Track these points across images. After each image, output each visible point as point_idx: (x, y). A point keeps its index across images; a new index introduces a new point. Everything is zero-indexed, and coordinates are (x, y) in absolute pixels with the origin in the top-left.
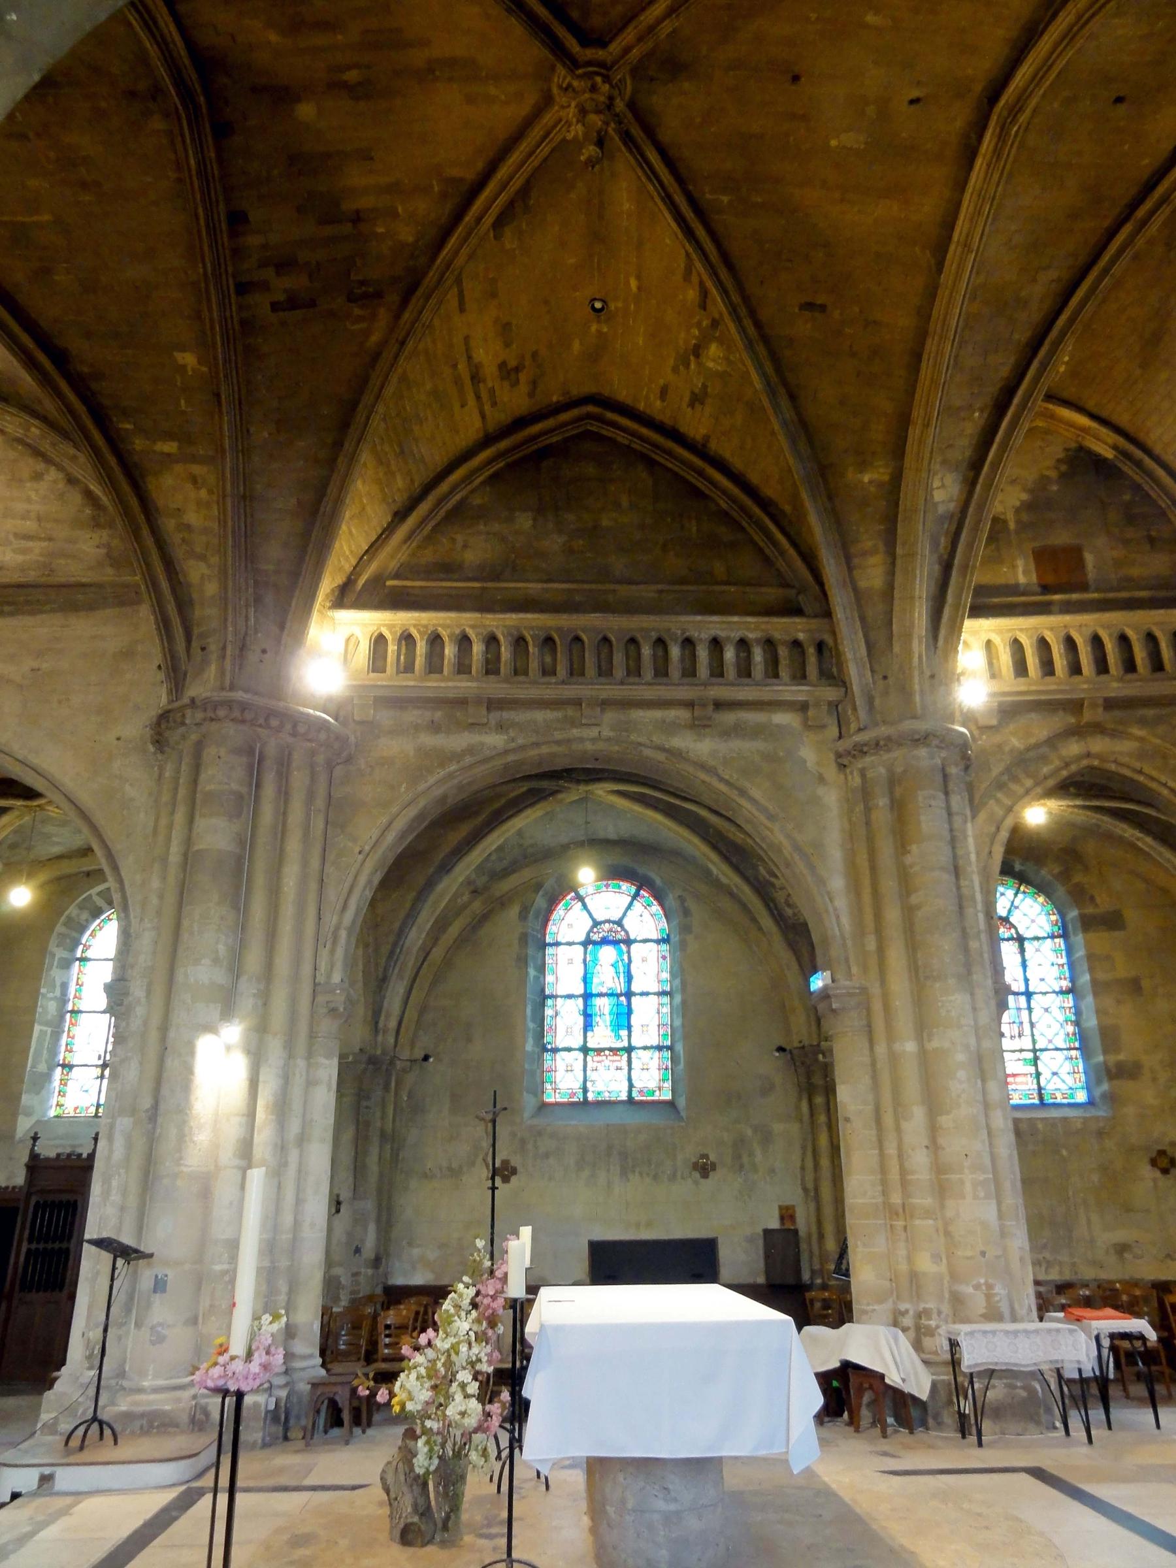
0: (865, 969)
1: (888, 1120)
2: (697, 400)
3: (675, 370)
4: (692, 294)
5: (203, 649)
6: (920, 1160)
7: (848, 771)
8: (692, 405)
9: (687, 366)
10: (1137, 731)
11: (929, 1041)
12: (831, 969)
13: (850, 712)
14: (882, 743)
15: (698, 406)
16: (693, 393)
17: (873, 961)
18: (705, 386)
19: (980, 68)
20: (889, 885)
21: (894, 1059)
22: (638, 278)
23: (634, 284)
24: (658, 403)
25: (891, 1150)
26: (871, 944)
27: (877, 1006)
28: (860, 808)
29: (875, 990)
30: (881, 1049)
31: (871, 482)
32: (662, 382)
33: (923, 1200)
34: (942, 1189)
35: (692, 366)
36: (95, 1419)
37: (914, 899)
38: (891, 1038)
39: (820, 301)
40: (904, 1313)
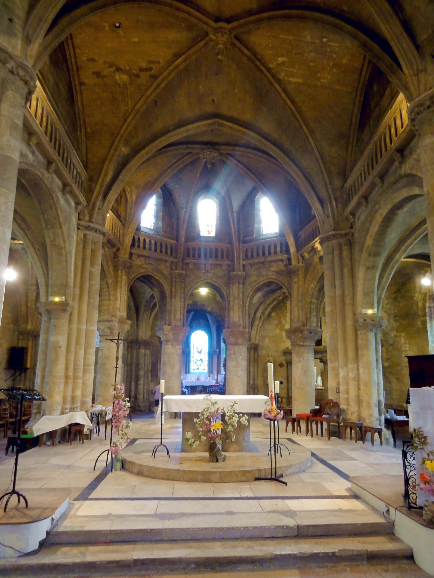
0: (73, 299)
1: (73, 349)
2: (98, 74)
3: (105, 63)
4: (144, 65)
5: (11, 20)
6: (82, 361)
7: (79, 231)
8: (94, 73)
9: (111, 66)
10: (107, 249)
11: (90, 326)
12: (65, 296)
13: (86, 213)
14: (98, 230)
15: (95, 76)
16: (99, 72)
17: (77, 297)
18: (106, 76)
19: (224, 111)
20: (87, 275)
21: (79, 330)
22: (138, 42)
23: (136, 40)
24: (85, 59)
25: (72, 358)
26: (77, 292)
27: (76, 312)
28: (81, 246)
29: (76, 307)
30: (74, 326)
31: (123, 152)
32: (96, 58)
33: (80, 374)
34: (85, 371)
35: (111, 69)
36: (14, 492)
37: (93, 282)
38: (79, 322)
39: (158, 104)
40: (66, 409)
